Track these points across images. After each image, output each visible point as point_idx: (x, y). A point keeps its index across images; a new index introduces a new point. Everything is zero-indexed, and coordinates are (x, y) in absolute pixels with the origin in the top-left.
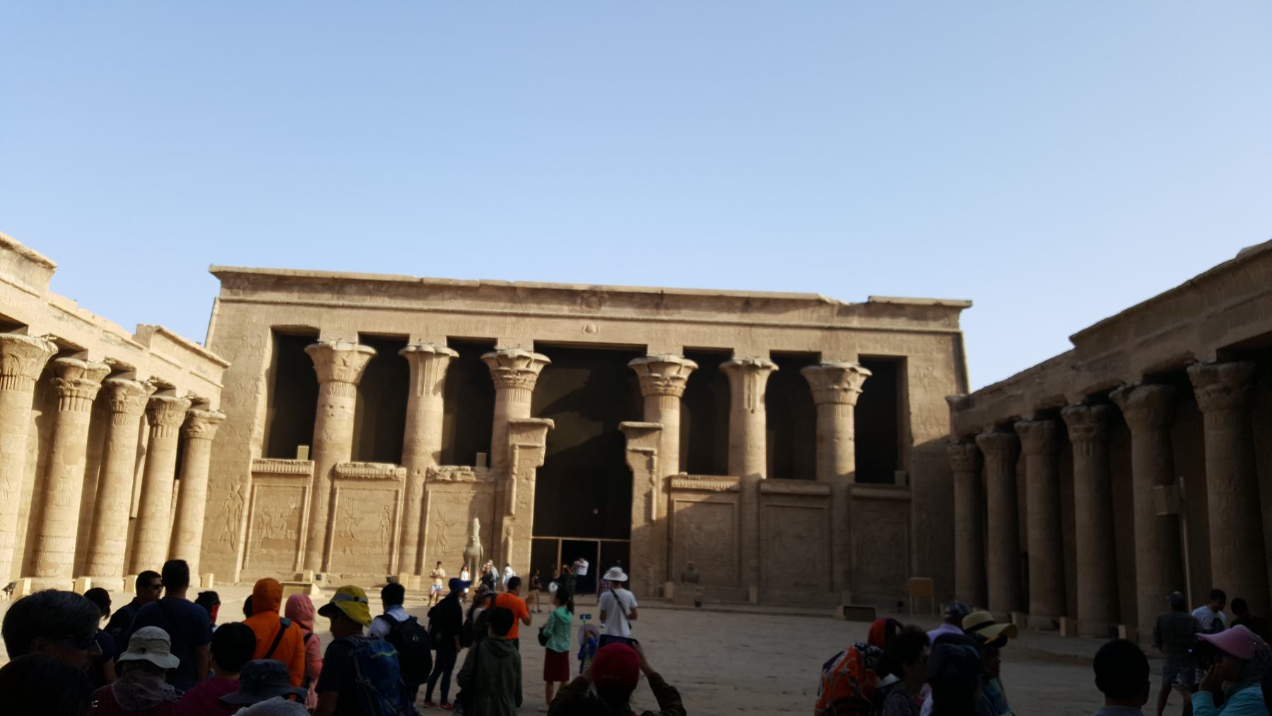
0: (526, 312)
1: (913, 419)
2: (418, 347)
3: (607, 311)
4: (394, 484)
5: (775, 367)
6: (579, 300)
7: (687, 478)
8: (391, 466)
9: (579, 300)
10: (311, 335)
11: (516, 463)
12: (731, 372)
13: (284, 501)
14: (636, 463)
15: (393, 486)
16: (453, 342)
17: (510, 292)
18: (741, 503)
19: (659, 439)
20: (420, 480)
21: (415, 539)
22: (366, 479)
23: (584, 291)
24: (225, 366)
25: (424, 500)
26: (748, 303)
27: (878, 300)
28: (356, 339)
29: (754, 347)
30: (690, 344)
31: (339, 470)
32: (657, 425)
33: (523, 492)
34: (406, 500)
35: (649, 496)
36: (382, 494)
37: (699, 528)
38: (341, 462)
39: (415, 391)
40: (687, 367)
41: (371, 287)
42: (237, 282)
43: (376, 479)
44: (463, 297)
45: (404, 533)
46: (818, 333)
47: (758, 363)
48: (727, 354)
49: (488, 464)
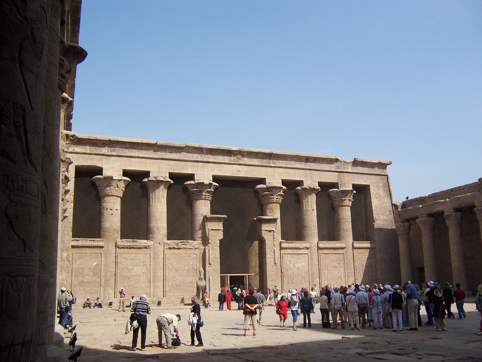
0: (208, 160)
1: (374, 212)
3: (246, 160)
4: (148, 250)
8: (146, 241)
17: (200, 150)
22: (134, 248)
23: (235, 151)
26: (307, 159)
29: (311, 180)
33: (214, 253)
36: (142, 255)
37: (294, 266)
44: (175, 152)
48: (300, 183)
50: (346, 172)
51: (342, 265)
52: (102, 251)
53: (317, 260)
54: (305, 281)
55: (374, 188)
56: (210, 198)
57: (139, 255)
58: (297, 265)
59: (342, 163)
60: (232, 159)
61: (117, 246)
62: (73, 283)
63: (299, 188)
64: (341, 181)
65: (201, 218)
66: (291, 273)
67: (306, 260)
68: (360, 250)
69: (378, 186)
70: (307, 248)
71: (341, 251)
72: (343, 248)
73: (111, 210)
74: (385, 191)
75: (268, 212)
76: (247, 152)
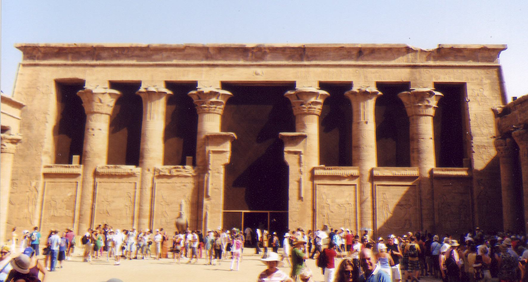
2: (146, 89)
5: (380, 93)
6: (250, 54)
7: (324, 169)
9: (250, 54)
10: (79, 84)
11: (211, 162)
12: (352, 98)
13: (64, 190)
14: (290, 160)
15: (132, 180)
16: (169, 85)
18: (361, 184)
19: (305, 144)
20: (149, 176)
21: (148, 214)
23: (253, 48)
24: (19, 106)
25: (153, 188)
26: (360, 53)
27: (445, 47)
28: (107, 85)
29: (364, 79)
31: (99, 170)
32: (304, 134)
33: (216, 181)
34: (141, 188)
35: (299, 182)
36: (125, 185)
38: (100, 165)
39: (146, 118)
40: (322, 95)
41: (117, 52)
42: (33, 53)
43: (122, 176)
45: (140, 210)
46: (408, 70)
47: (368, 90)
48: (348, 85)
49: (194, 164)
52: (80, 180)
55: (473, 87)
56: (221, 111)
57: (122, 184)
59: (418, 54)
61: (96, 174)
62: (43, 218)
63: (347, 93)
65: (203, 136)
66: (329, 212)
67: (353, 193)
69: (480, 84)
73: (93, 129)
74: (492, 89)
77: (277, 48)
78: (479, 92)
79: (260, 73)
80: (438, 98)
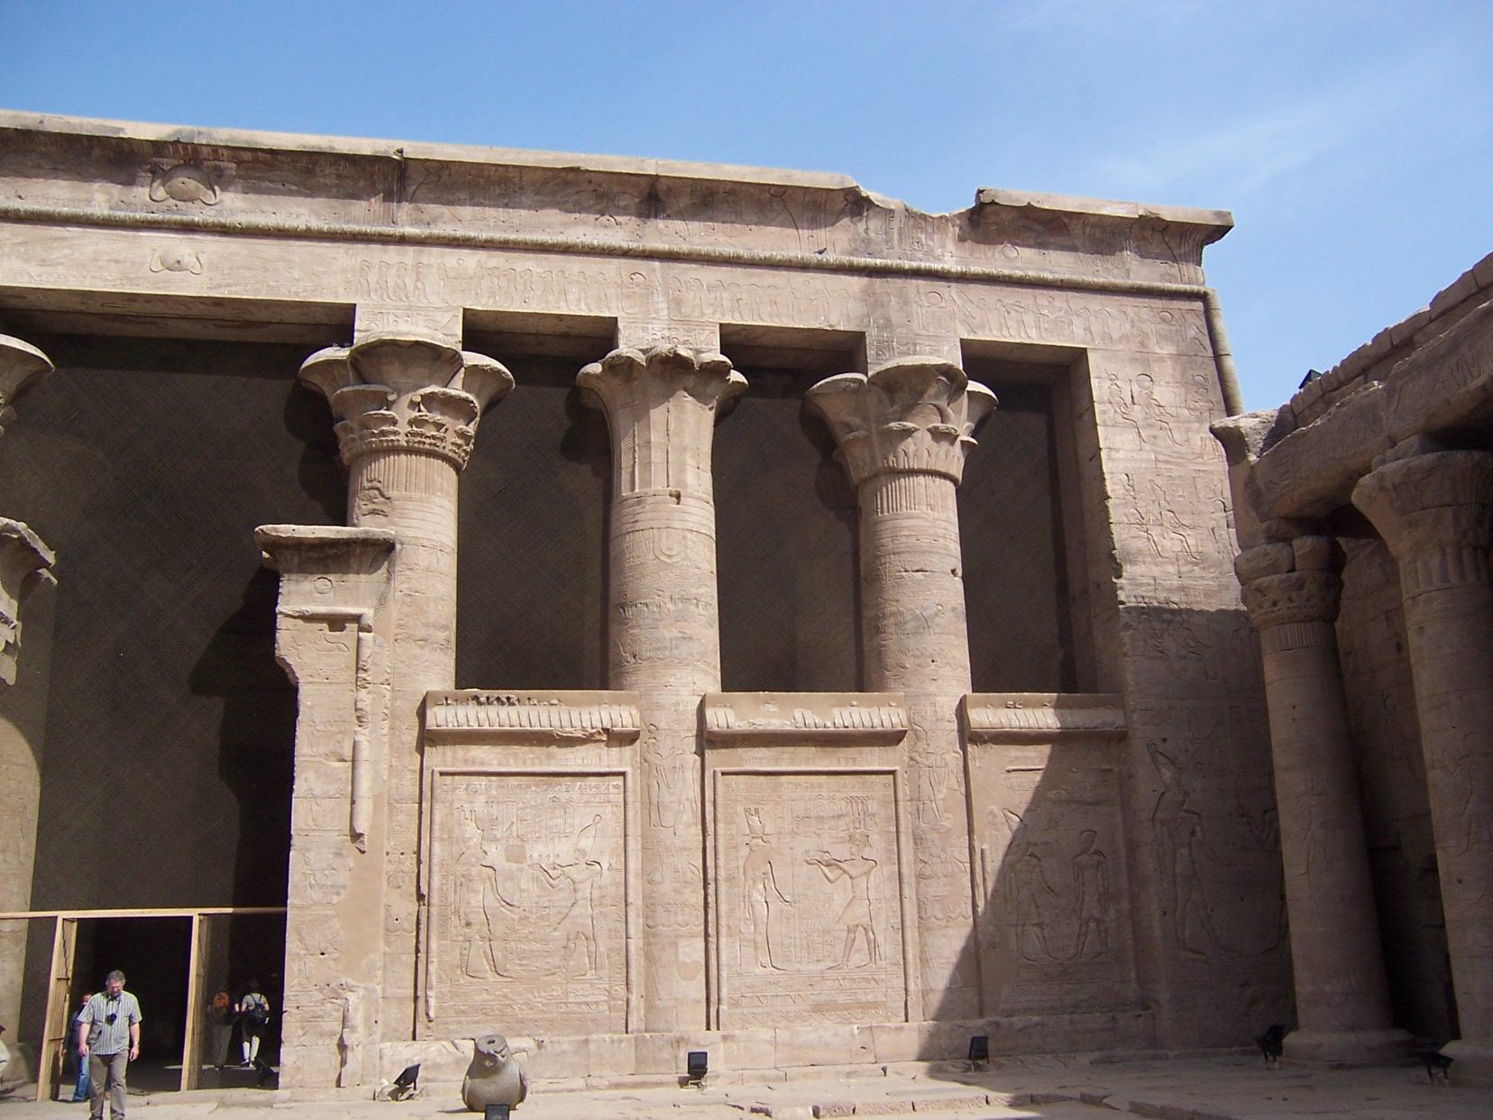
1: (1118, 513)
3: (233, 205)
5: (736, 376)
26: (654, 197)
29: (669, 307)
30: (480, 305)
37: (516, 855)
40: (475, 369)
47: (683, 352)
50: (917, 274)
51: (878, 846)
53: (690, 815)
54: (593, 957)
55: (1113, 368)
58: (537, 851)
59: (895, 225)
60: (142, 197)
63: (595, 368)
64: (888, 325)
66: (492, 902)
67: (611, 815)
68: (1014, 751)
69: (1143, 358)
70: (624, 739)
71: (873, 758)
72: (890, 738)
75: (360, 506)
76: (235, 152)
77: (272, 152)
78: (1136, 388)
79: (189, 260)
80: (979, 410)
